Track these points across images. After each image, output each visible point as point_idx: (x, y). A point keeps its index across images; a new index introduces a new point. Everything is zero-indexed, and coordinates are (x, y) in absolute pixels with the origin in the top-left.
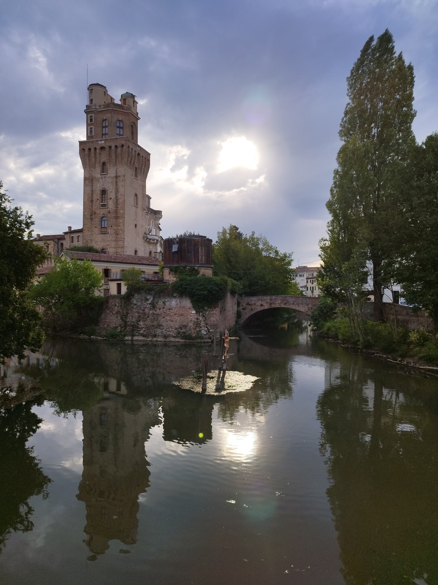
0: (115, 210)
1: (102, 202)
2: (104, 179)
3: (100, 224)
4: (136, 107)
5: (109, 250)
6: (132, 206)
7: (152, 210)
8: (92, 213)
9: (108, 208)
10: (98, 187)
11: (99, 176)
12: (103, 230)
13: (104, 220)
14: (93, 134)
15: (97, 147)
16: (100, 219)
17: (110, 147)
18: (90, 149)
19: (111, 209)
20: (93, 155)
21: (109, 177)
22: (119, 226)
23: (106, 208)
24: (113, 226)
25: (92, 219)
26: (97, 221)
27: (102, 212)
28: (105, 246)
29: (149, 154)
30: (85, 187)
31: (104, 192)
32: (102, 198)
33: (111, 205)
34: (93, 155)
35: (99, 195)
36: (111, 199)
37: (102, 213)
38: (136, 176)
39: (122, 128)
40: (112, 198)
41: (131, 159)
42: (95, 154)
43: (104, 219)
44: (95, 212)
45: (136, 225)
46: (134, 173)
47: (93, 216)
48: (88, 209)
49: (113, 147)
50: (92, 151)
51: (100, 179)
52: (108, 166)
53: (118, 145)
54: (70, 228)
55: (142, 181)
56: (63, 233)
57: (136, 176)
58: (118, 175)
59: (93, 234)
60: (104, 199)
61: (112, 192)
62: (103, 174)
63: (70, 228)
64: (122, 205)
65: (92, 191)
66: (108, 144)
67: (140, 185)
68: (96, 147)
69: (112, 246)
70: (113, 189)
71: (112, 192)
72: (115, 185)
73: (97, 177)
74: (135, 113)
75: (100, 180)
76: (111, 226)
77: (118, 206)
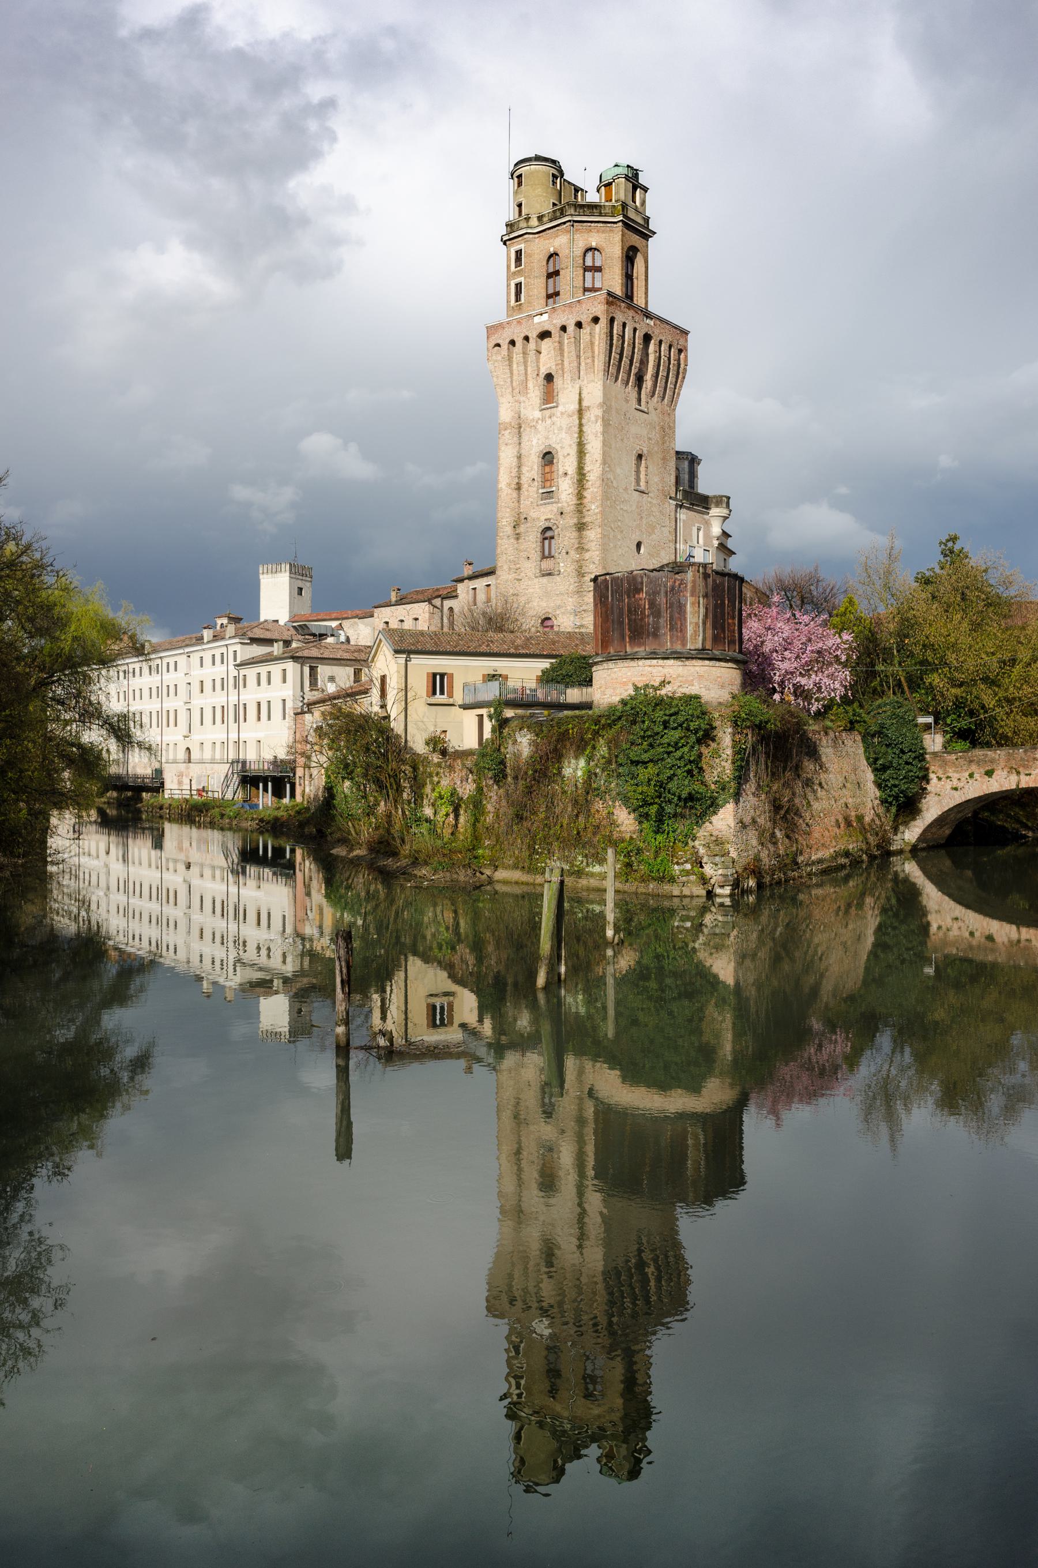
0: (578, 505)
2: (549, 421)
3: (538, 549)
4: (643, 203)
5: (561, 621)
7: (698, 494)
8: (519, 518)
10: (534, 445)
11: (537, 414)
12: (547, 564)
15: (530, 335)
17: (564, 329)
18: (513, 343)
19: (565, 504)
21: (562, 413)
22: (587, 550)
23: (556, 503)
25: (518, 536)
26: (532, 540)
27: (542, 514)
28: (550, 611)
29: (685, 333)
31: (548, 457)
33: (565, 488)
35: (536, 467)
37: (543, 518)
39: (599, 269)
40: (569, 473)
43: (549, 534)
44: (525, 516)
47: (522, 529)
48: (508, 510)
49: (571, 328)
51: (540, 422)
52: (558, 381)
53: (585, 319)
59: (520, 578)
61: (568, 454)
64: (595, 490)
65: (519, 457)
66: (559, 322)
68: (527, 334)
69: (569, 608)
70: (570, 445)
71: (568, 454)
72: (576, 435)
73: (531, 417)
74: (641, 222)
75: (540, 426)
76: (567, 553)
77: (585, 494)
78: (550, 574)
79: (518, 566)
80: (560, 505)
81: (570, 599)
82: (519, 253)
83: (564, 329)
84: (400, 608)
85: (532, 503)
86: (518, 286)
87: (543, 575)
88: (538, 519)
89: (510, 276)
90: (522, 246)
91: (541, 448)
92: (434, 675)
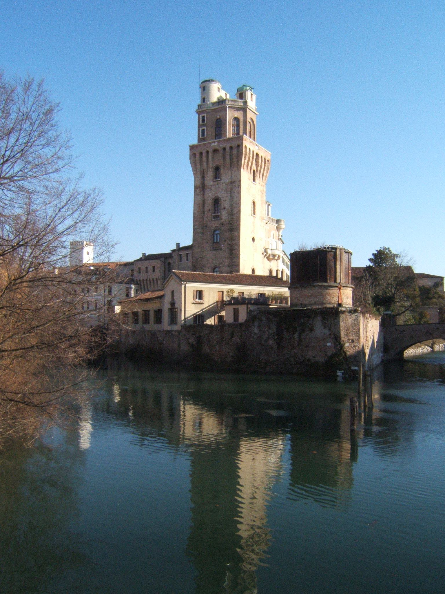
1: (215, 213)
6: (249, 215)
9: (220, 220)
10: (210, 195)
11: (211, 183)
12: (216, 245)
13: (217, 234)
14: (205, 136)
16: (212, 233)
17: (224, 149)
18: (201, 153)
19: (224, 221)
20: (204, 159)
21: (223, 183)
24: (227, 241)
27: (215, 224)
28: (217, 264)
30: (196, 196)
31: (216, 201)
32: (215, 208)
33: (224, 214)
34: (204, 159)
36: (224, 208)
37: (214, 226)
38: (254, 180)
41: (249, 161)
42: (207, 157)
43: (217, 232)
45: (253, 239)
46: (252, 178)
48: (198, 222)
49: (228, 149)
50: (204, 154)
52: (222, 170)
54: (178, 244)
55: (262, 185)
56: (171, 251)
57: (254, 180)
58: (233, 180)
60: (216, 209)
61: (226, 200)
62: (216, 181)
63: (178, 244)
66: (222, 146)
67: (258, 191)
68: (208, 150)
71: (226, 200)
75: (213, 188)
76: (225, 241)
78: (217, 250)
79: (202, 245)
80: (222, 221)
81: (226, 260)
82: (203, 117)
83: (224, 149)
84: (147, 262)
85: (209, 219)
86: (203, 130)
87: (214, 250)
88: (212, 226)
89: (199, 126)
90: (205, 115)
91: (213, 197)
92: (197, 291)
